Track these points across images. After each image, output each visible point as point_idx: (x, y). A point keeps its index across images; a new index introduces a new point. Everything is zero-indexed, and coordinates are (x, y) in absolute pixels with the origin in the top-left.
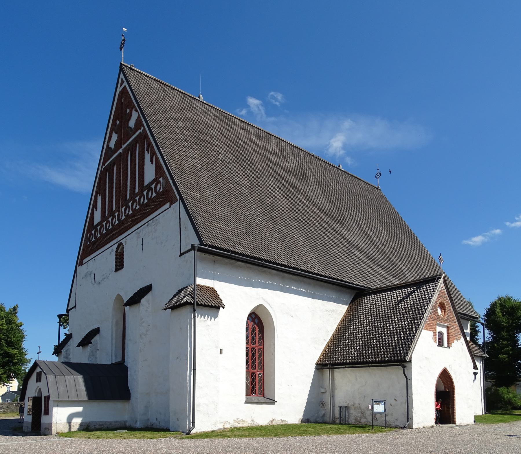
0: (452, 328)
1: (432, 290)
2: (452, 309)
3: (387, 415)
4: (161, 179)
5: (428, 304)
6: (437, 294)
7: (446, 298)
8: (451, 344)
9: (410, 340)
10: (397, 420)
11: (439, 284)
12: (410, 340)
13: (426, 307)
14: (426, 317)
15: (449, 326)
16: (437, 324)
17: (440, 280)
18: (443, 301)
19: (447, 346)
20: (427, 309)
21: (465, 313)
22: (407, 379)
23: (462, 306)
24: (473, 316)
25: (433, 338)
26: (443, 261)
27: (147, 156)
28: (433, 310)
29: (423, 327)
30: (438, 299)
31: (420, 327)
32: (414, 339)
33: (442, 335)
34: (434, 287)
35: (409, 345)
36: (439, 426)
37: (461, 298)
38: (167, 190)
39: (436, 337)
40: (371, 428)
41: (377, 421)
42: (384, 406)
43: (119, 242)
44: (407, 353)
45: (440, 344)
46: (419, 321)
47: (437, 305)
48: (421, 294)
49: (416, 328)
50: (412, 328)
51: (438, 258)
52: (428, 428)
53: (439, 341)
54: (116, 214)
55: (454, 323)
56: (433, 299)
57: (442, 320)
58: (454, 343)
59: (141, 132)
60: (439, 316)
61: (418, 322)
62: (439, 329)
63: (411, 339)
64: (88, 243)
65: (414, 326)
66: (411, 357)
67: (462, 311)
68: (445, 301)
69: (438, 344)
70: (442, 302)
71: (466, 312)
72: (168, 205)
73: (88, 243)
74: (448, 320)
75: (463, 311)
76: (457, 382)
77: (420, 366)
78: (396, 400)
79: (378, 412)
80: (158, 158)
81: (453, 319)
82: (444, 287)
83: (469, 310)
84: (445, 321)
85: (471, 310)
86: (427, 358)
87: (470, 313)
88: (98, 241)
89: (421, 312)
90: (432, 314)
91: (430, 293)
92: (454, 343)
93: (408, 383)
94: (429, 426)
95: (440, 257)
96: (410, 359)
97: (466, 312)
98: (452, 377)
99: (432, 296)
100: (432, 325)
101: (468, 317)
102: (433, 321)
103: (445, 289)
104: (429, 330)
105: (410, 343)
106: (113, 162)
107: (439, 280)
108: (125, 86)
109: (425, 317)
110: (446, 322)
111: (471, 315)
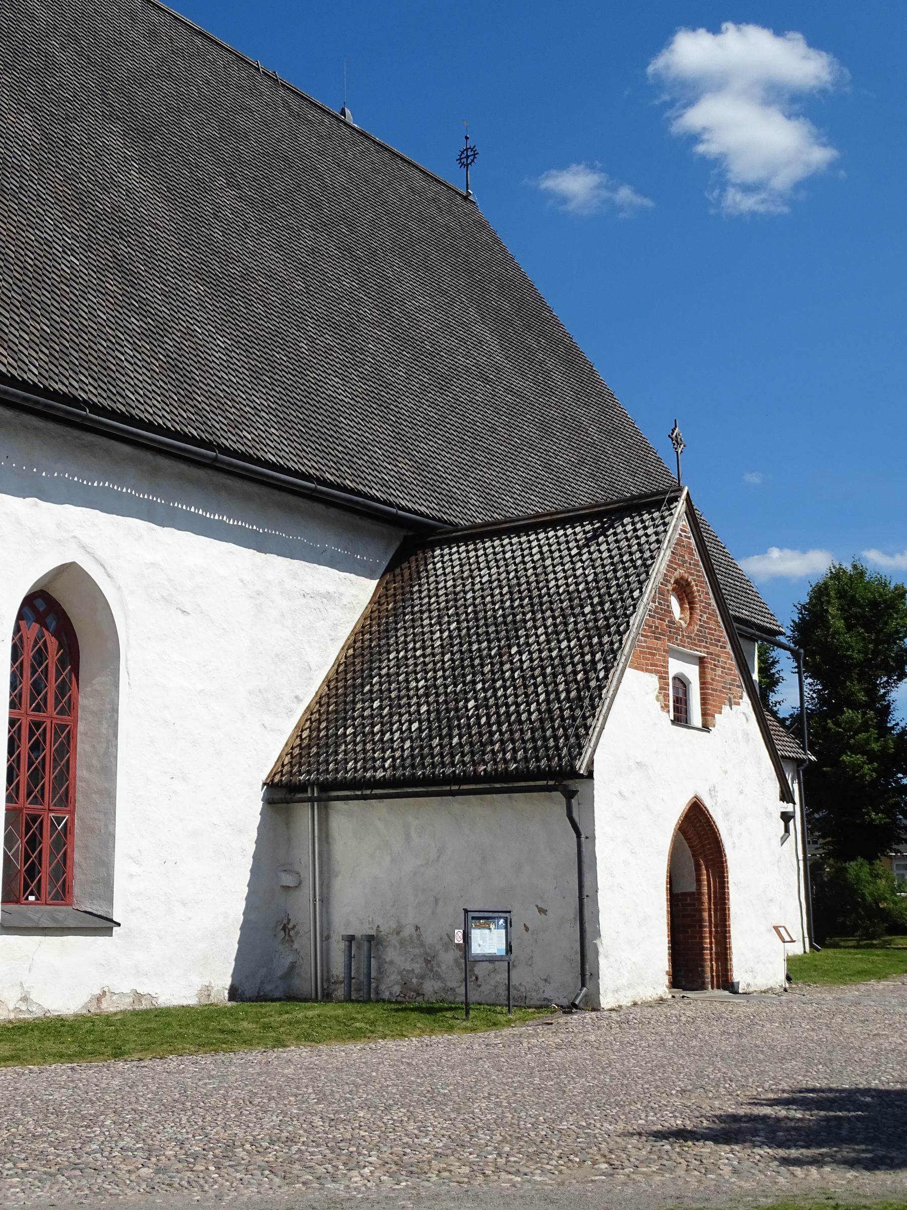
0: (715, 665)
1: (653, 538)
2: (713, 602)
3: (514, 966)
5: (641, 583)
6: (669, 552)
7: (694, 564)
8: (714, 717)
9: (587, 702)
10: (546, 980)
11: (675, 520)
12: (587, 702)
13: (636, 594)
14: (636, 626)
15: (704, 657)
16: (672, 649)
17: (676, 507)
18: (686, 575)
19: (700, 725)
20: (638, 598)
21: (743, 616)
22: (579, 835)
23: (733, 594)
24: (768, 625)
25: (657, 696)
26: (682, 446)
28: (657, 604)
29: (627, 660)
30: (671, 567)
31: (618, 657)
32: (601, 698)
33: (685, 686)
34: (657, 526)
35: (585, 718)
36: (683, 997)
37: (731, 569)
39: (668, 695)
40: (461, 1014)
41: (479, 986)
42: (503, 931)
44: (581, 747)
45: (681, 718)
46: (616, 638)
47: (670, 587)
48: (619, 548)
49: (605, 661)
50: (594, 662)
51: (669, 436)
52: (648, 1005)
53: (678, 707)
55: (721, 647)
56: (656, 566)
57: (683, 636)
58: (720, 713)
60: (674, 623)
61: (612, 643)
62: (676, 667)
63: (592, 699)
65: (598, 656)
66: (591, 762)
67: (736, 611)
68: (692, 574)
69: (674, 716)
70: (682, 578)
71: (747, 613)
74: (702, 636)
75: (737, 609)
76: (734, 843)
77: (620, 793)
78: (542, 911)
79: (484, 956)
81: (718, 636)
82: (688, 529)
83: (755, 607)
84: (695, 639)
85: (761, 609)
86: (641, 762)
87: (759, 617)
89: (622, 607)
90: (653, 617)
91: (647, 547)
92: (720, 713)
93: (584, 849)
94: (650, 999)
95: (673, 431)
96: (587, 766)
97: (747, 613)
98: (719, 827)
99: (652, 558)
100: (654, 655)
101: (753, 631)
102: (656, 638)
103: (690, 535)
104: (647, 671)
105: (588, 714)
107: (672, 506)
109: (634, 625)
110: (696, 645)
111: (762, 623)
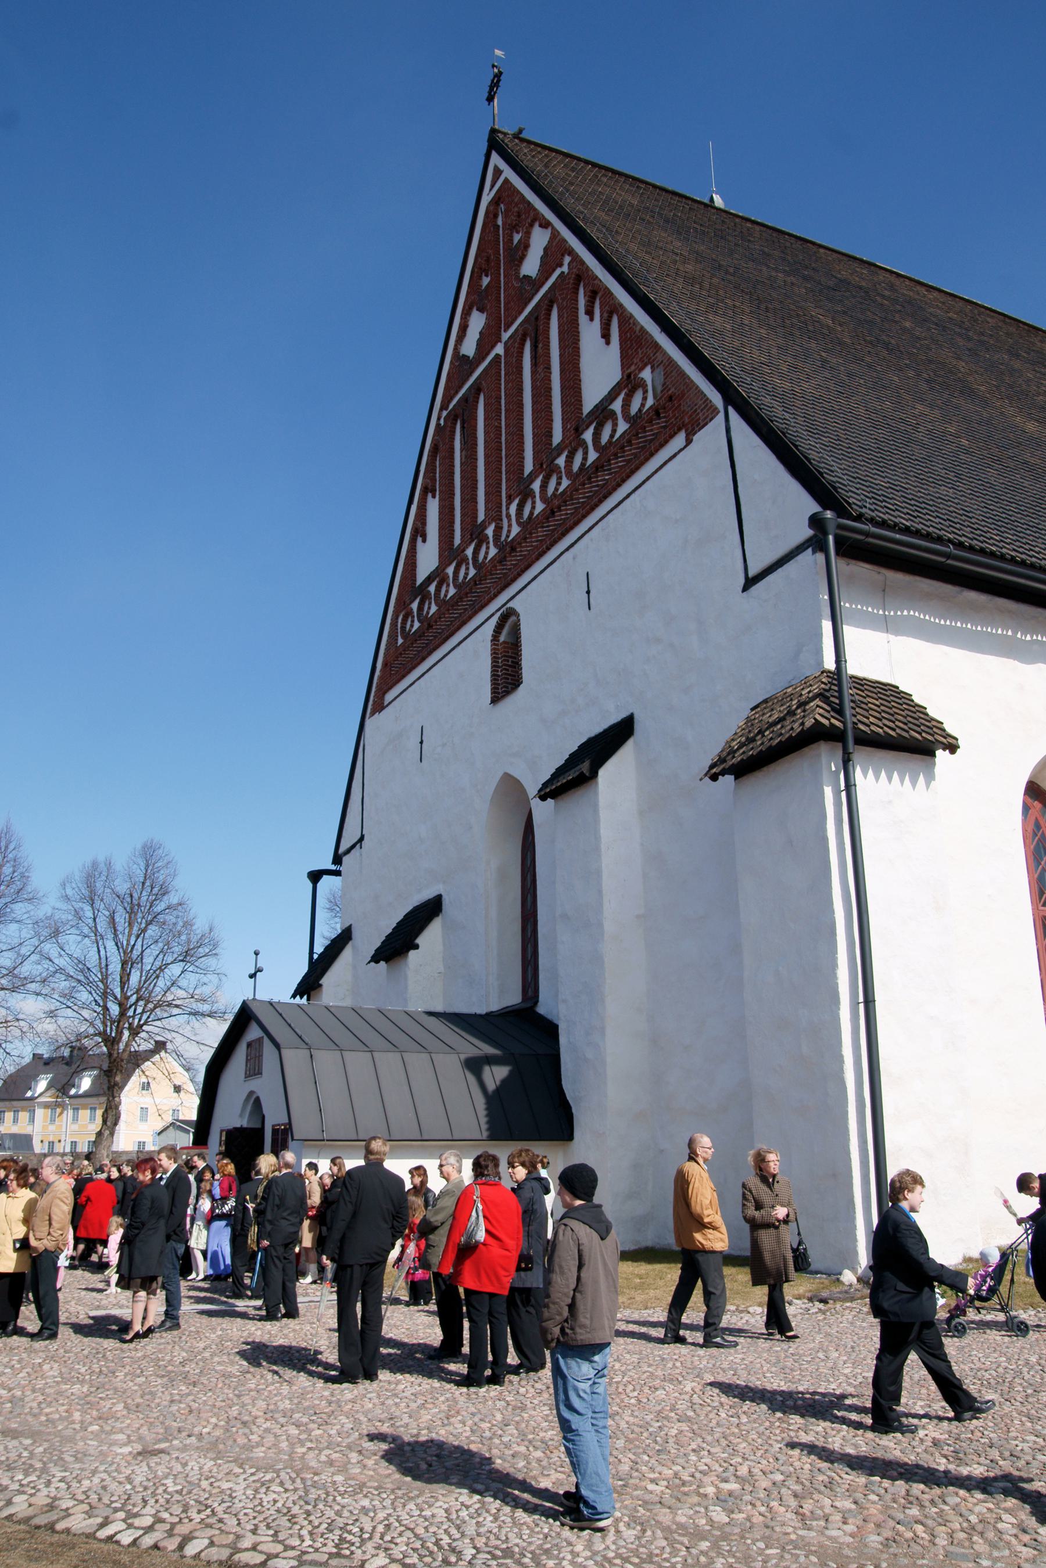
4: (646, 374)
27: (589, 331)
38: (670, 398)
43: (504, 609)
54: (490, 531)
59: (563, 273)
64: (400, 641)
72: (680, 440)
73: (400, 641)
80: (631, 316)
88: (430, 626)
106: (477, 389)
108: (506, 181)
